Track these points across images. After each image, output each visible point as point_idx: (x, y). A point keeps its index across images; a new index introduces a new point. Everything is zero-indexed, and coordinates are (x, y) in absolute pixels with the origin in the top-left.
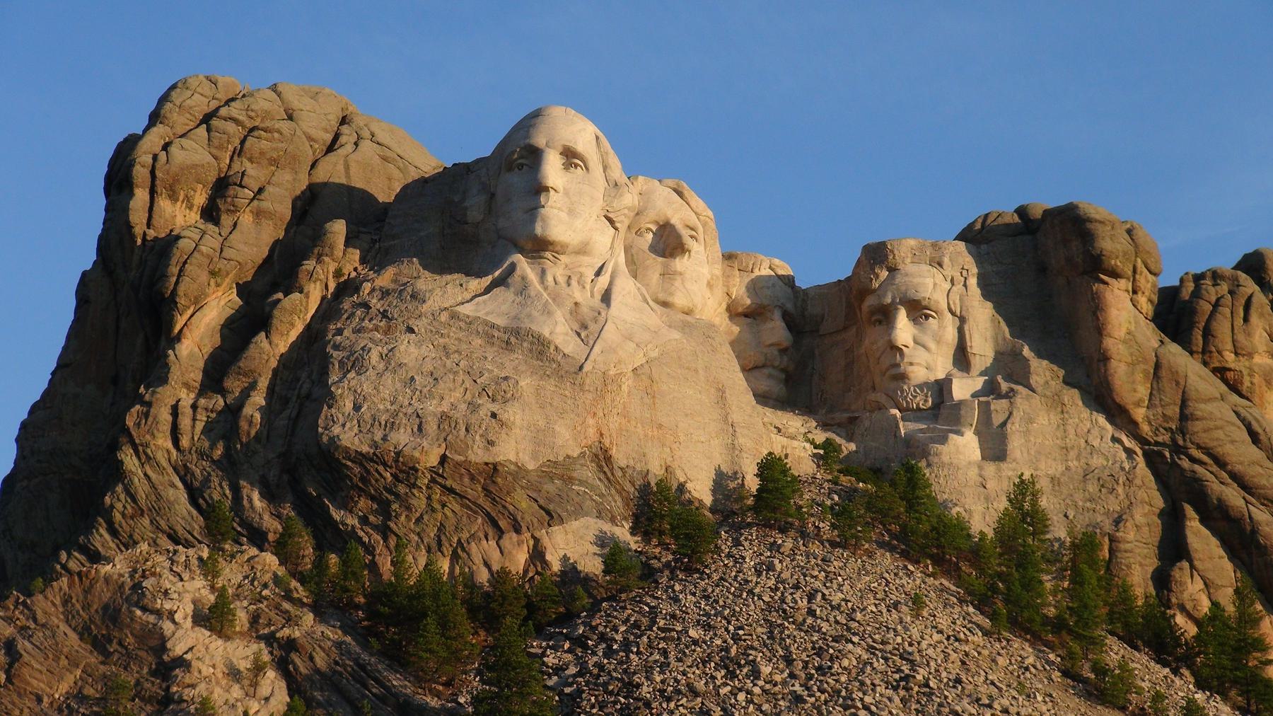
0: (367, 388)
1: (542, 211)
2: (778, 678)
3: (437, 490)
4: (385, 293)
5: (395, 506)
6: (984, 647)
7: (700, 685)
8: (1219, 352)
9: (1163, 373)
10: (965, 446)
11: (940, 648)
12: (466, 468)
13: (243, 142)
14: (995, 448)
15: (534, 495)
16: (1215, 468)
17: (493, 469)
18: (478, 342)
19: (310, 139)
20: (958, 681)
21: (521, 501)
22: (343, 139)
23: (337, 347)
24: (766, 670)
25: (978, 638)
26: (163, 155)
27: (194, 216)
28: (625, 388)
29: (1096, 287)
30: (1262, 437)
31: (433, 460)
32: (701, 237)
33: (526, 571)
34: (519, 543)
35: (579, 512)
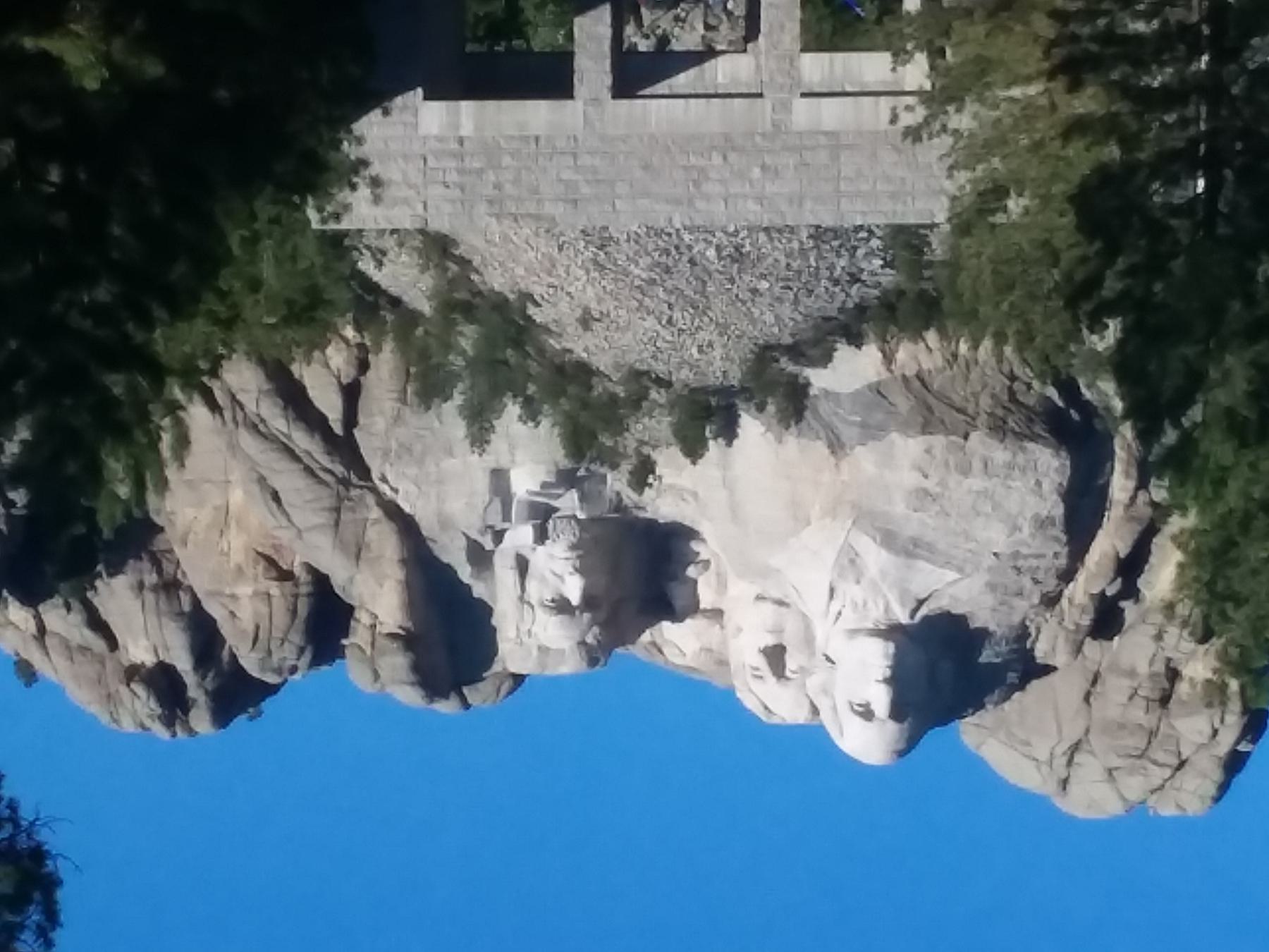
0: (1032, 500)
1: (890, 663)
2: (702, 245)
3: (971, 411)
4: (1020, 594)
5: (1006, 398)
6: (534, 283)
7: (762, 237)
8: (283, 594)
9: (354, 549)
10: (526, 482)
11: (571, 278)
12: (948, 432)
13: (1149, 742)
14: (499, 479)
15: (892, 409)
16: (314, 466)
17: (926, 429)
18: (941, 546)
19: (1092, 753)
20: (560, 248)
21: (903, 403)
22: (1064, 760)
23: (1057, 539)
24: (711, 253)
25: (538, 291)
26: (1217, 725)
27: (1187, 671)
28: (817, 507)
29: (409, 625)
30: (269, 497)
31: (975, 436)
32: (749, 672)
33: (898, 344)
34: (903, 366)
35: (856, 394)
